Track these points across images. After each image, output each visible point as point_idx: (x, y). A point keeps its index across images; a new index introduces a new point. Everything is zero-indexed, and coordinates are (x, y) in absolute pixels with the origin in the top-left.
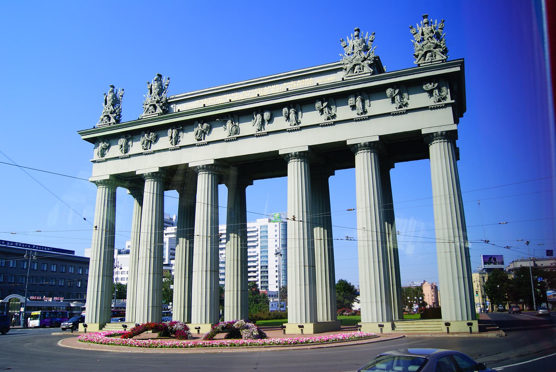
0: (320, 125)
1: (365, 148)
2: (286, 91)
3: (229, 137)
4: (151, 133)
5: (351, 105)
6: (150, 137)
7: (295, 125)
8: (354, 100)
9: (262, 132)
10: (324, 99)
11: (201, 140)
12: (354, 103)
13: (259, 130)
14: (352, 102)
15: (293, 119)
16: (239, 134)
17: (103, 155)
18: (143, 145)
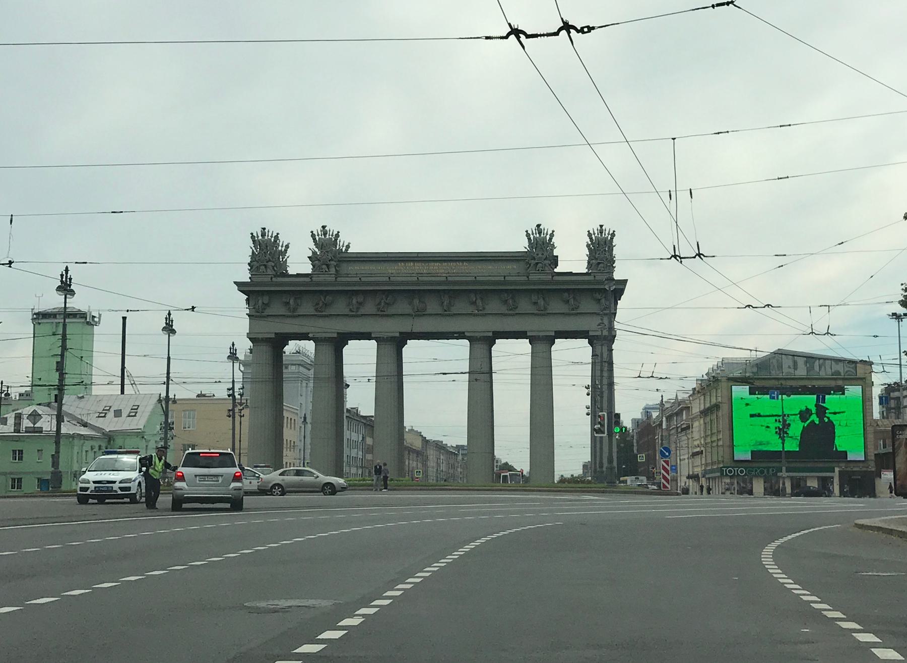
11: (384, 311)
13: (445, 311)
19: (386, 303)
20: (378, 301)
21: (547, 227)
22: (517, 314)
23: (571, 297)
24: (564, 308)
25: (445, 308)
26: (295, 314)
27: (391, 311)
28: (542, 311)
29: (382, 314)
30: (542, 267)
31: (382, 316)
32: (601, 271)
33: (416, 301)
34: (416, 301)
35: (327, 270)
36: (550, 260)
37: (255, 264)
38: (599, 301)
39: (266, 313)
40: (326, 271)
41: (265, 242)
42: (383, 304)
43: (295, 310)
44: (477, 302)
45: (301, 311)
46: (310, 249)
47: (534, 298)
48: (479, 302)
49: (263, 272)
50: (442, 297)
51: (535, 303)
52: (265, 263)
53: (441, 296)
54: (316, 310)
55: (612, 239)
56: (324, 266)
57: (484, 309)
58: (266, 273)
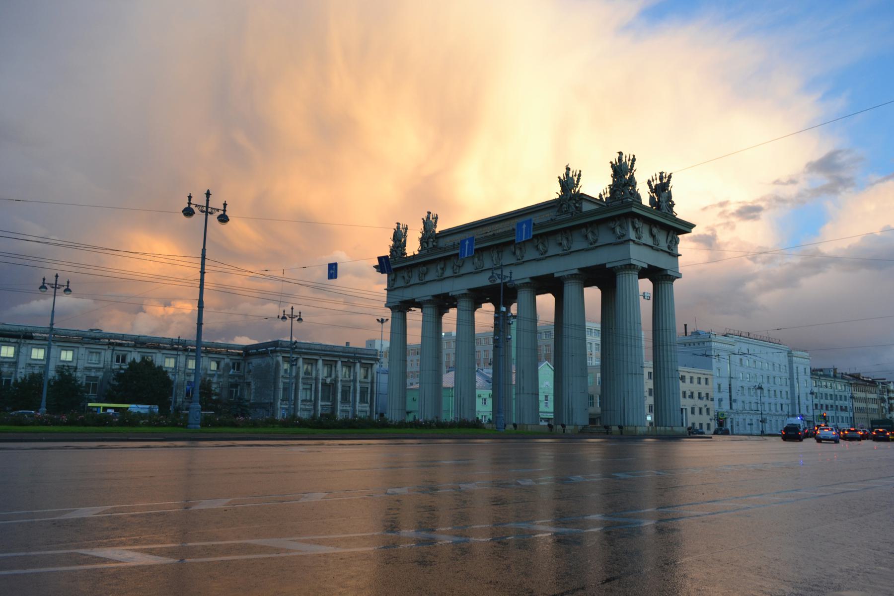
13: (495, 265)
19: (457, 266)
21: (574, 168)
22: (546, 257)
23: (588, 231)
24: (610, 238)
25: (495, 263)
26: (408, 284)
28: (566, 250)
31: (456, 277)
36: (575, 200)
38: (613, 230)
47: (559, 238)
51: (560, 244)
54: (420, 280)
55: (633, 164)
57: (522, 257)
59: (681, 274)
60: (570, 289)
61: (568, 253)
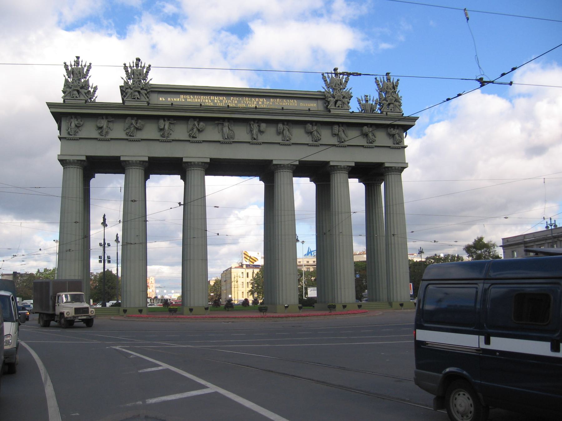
0: (309, 145)
1: (344, 170)
2: (226, 107)
3: (226, 140)
4: (139, 121)
5: (335, 133)
6: (138, 125)
7: (287, 141)
8: (338, 130)
9: (258, 141)
10: (314, 124)
11: (196, 138)
12: (337, 132)
13: (255, 139)
14: (335, 131)
15: (286, 135)
16: (233, 139)
17: (76, 133)
18: (128, 131)
20: (190, 127)
27: (201, 137)
29: (192, 140)
30: (341, 105)
32: (393, 111)
33: (226, 130)
34: (226, 130)
35: (139, 97)
37: (68, 88)
39: (78, 136)
40: (138, 99)
41: (78, 70)
42: (195, 130)
43: (107, 133)
44: (284, 132)
45: (112, 135)
46: (122, 78)
48: (286, 133)
49: (76, 97)
50: (252, 125)
52: (79, 89)
53: (250, 125)
54: (127, 134)
56: (137, 93)
58: (79, 98)
59: (181, 179)
60: (282, 177)
61: (341, 144)
